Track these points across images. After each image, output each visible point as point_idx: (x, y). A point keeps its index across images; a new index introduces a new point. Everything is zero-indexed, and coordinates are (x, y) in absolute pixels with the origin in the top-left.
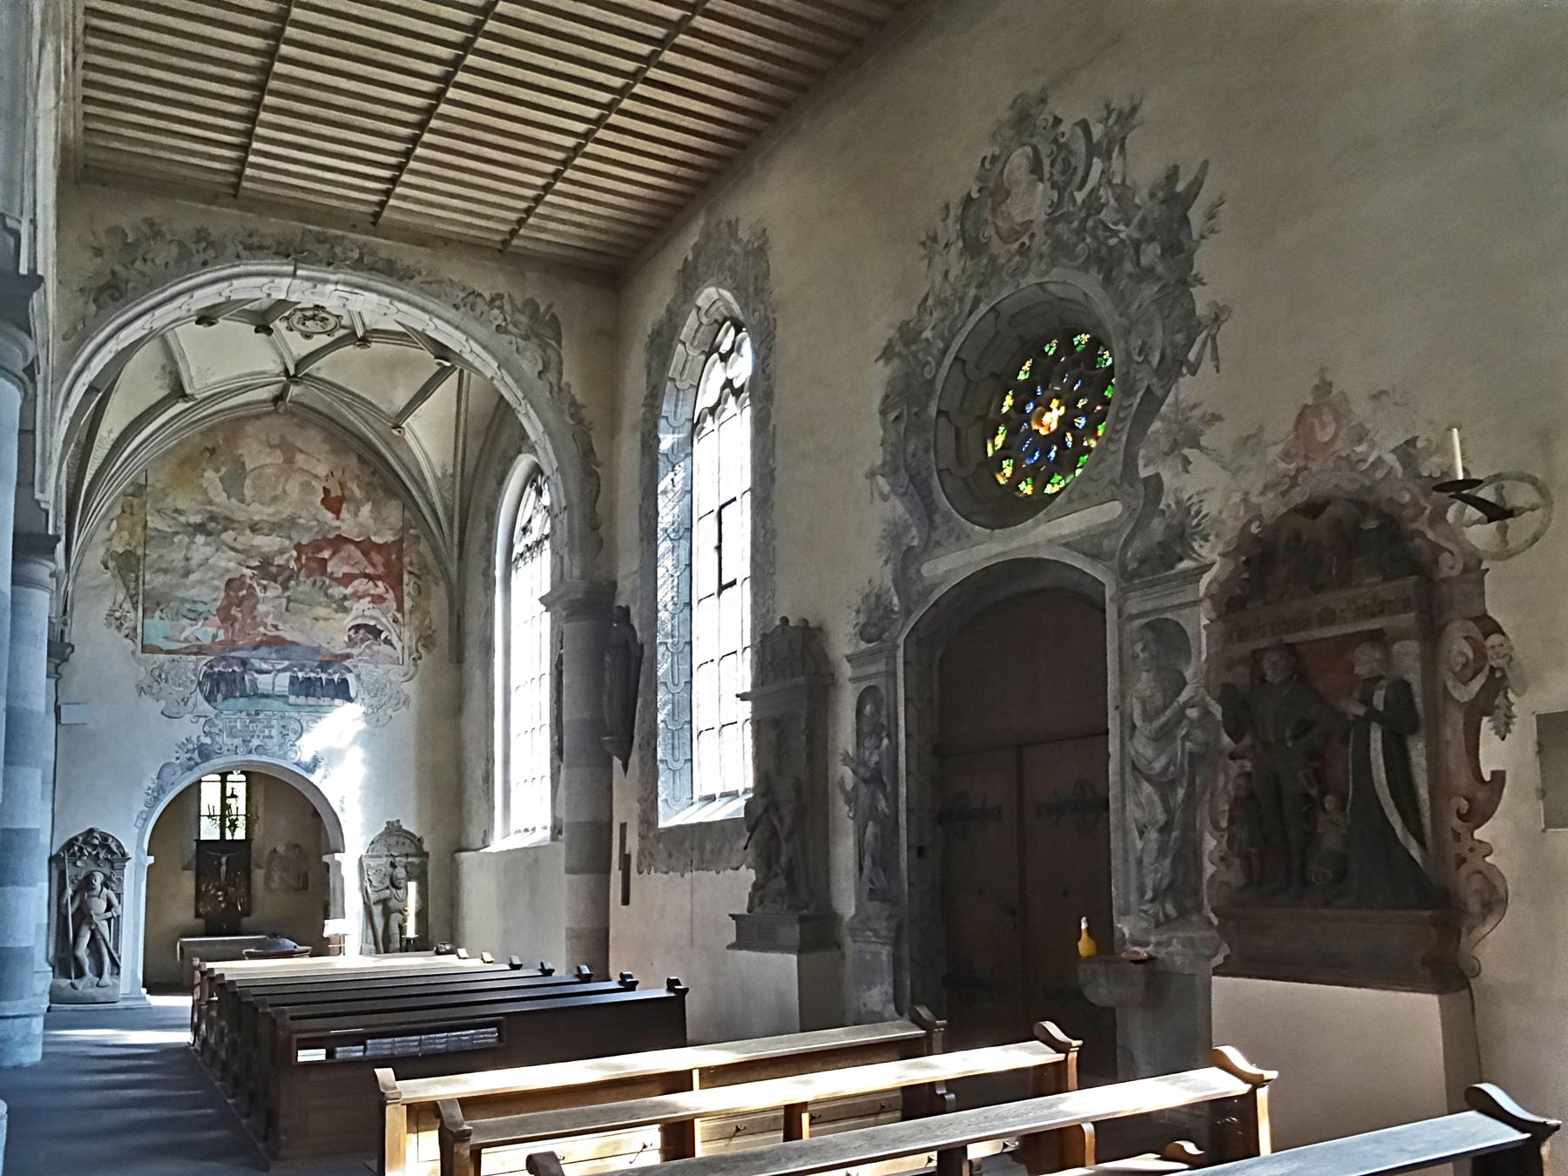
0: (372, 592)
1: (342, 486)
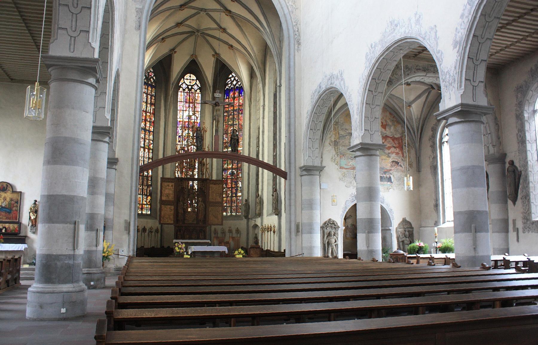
0: (395, 151)
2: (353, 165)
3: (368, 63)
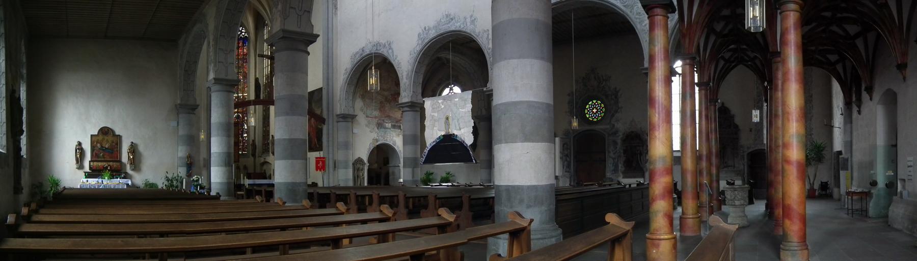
3: (420, 42)
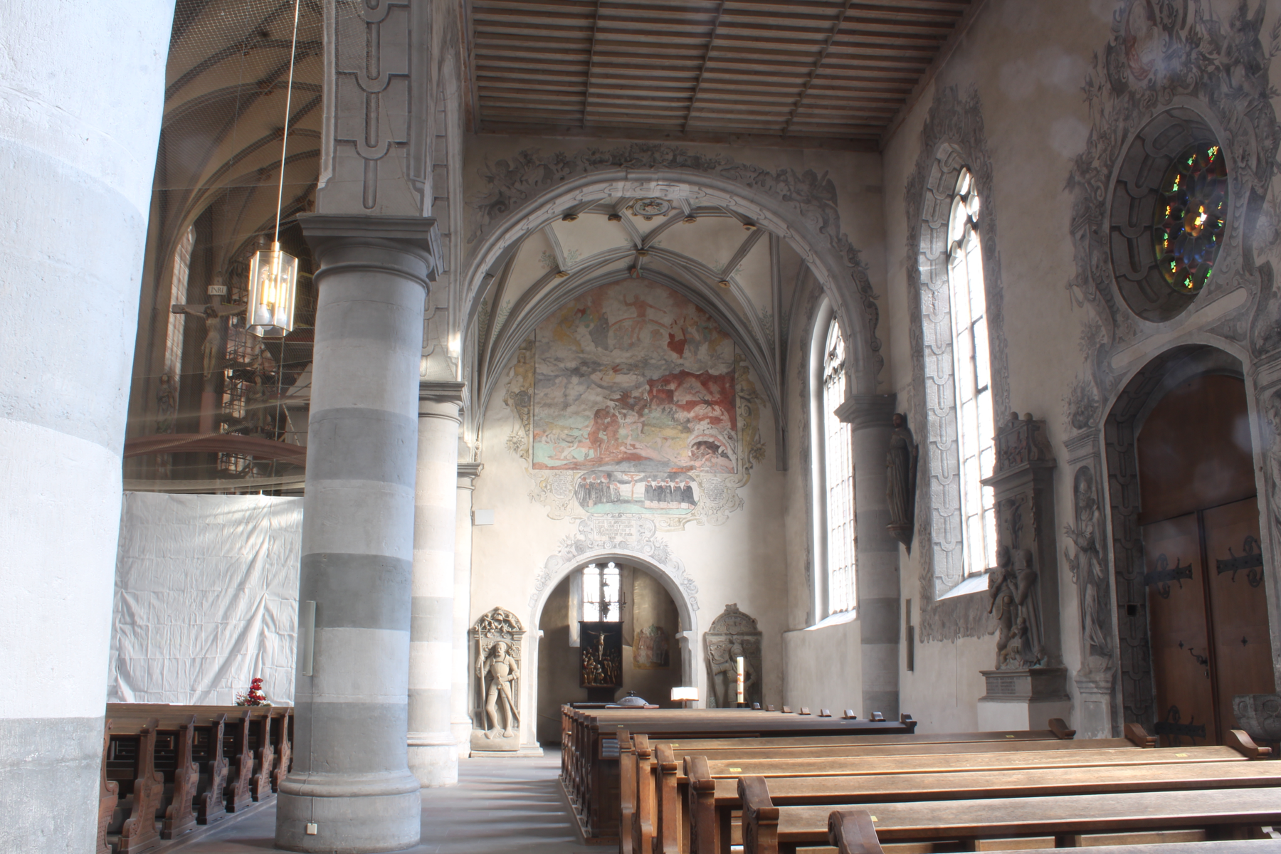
0: (711, 415)
1: (684, 331)
2: (574, 458)
